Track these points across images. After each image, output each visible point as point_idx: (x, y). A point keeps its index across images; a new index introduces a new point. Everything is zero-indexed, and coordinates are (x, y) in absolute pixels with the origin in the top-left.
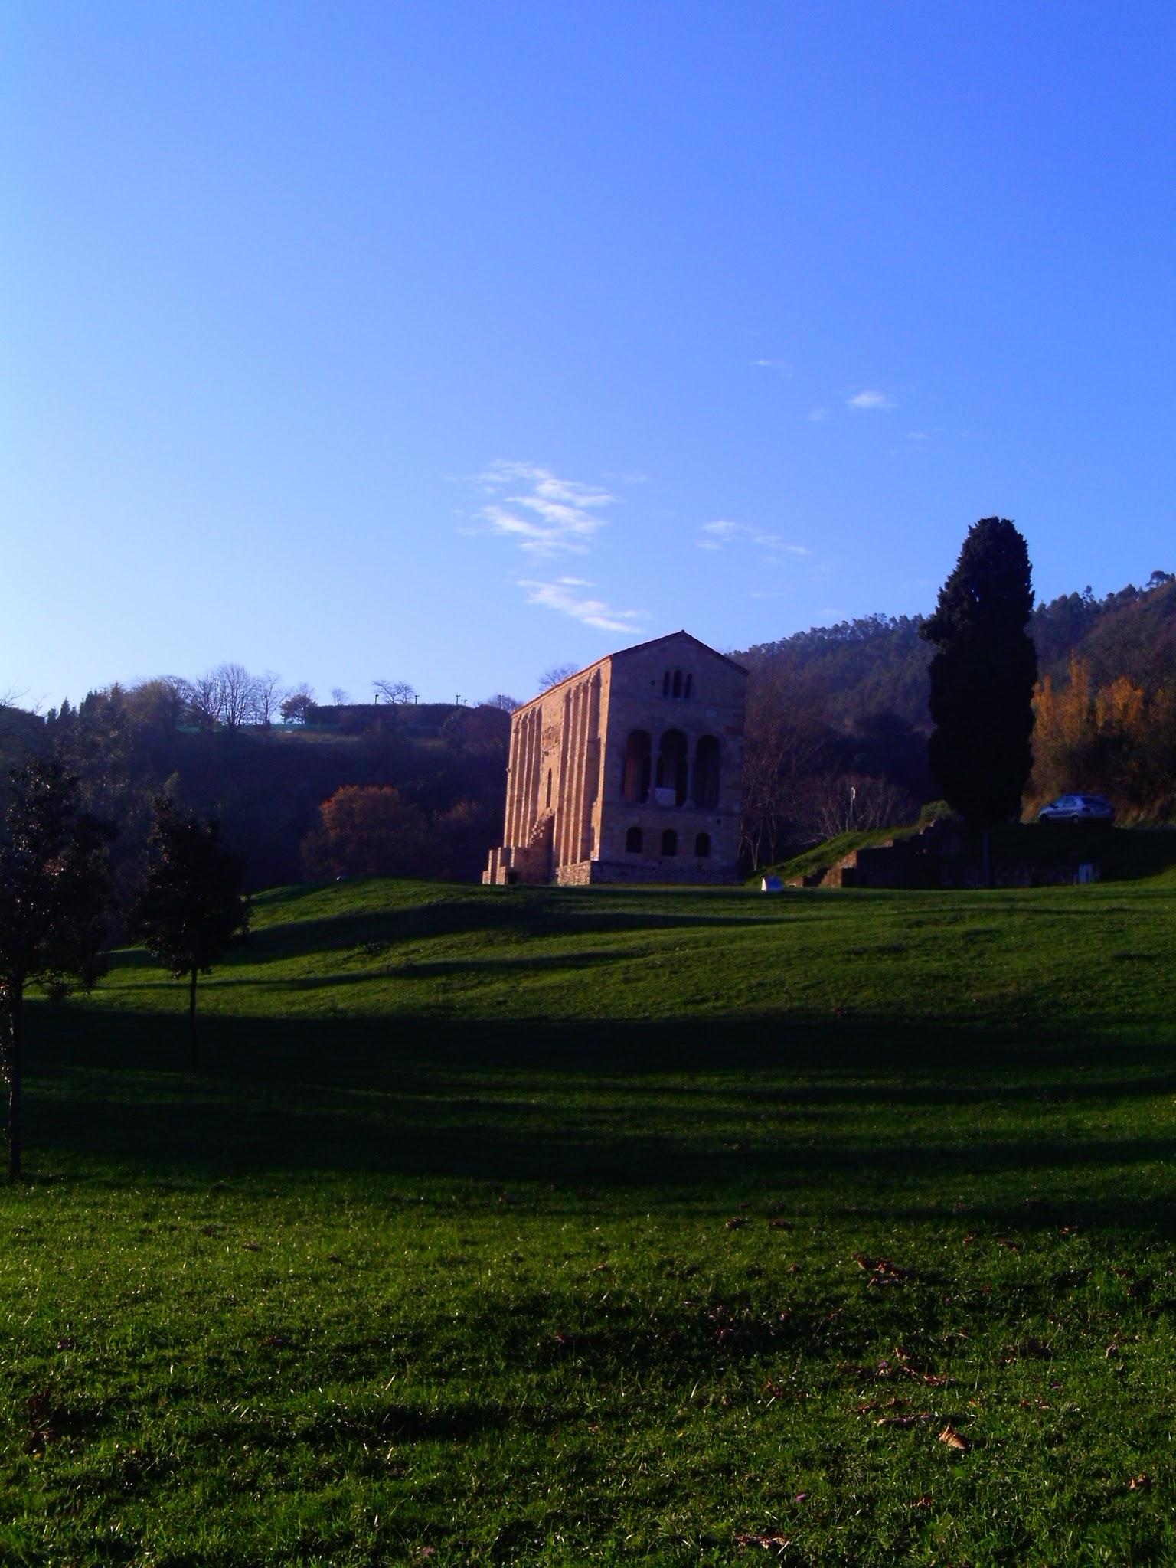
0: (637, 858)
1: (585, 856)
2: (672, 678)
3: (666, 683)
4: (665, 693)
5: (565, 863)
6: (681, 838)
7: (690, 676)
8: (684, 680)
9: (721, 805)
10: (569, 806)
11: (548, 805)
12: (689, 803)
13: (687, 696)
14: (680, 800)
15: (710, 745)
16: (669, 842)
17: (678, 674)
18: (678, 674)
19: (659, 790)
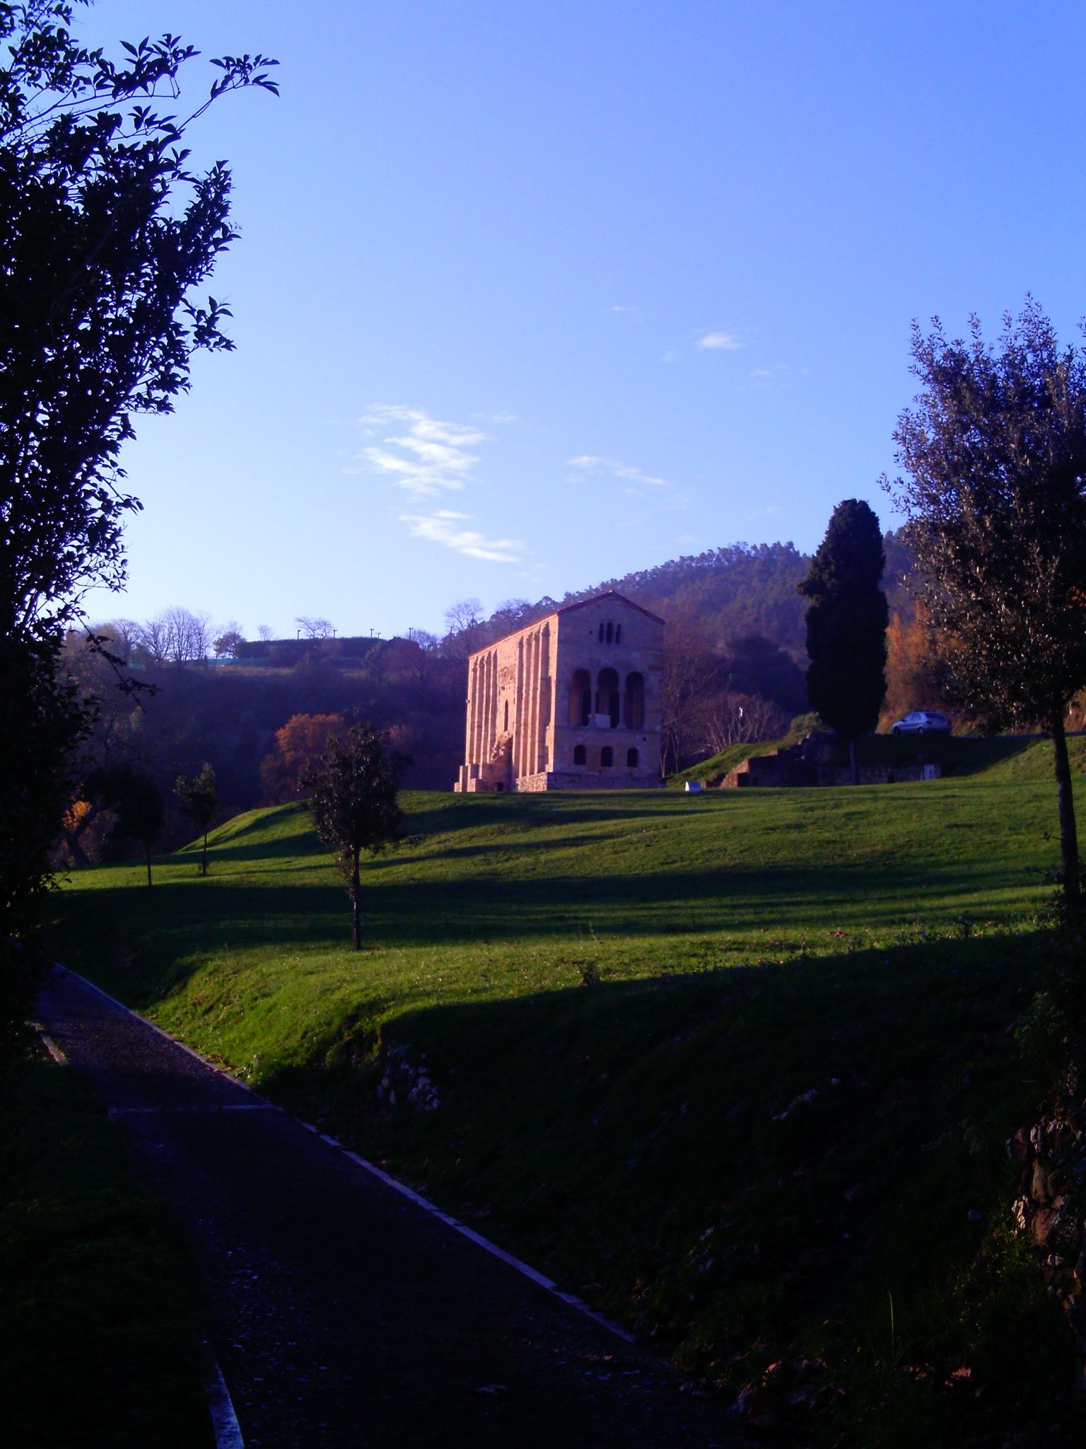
0: (582, 769)
1: (541, 769)
2: (605, 628)
3: (601, 632)
4: (601, 640)
5: (524, 774)
6: (615, 753)
7: (619, 626)
8: (615, 629)
9: (646, 727)
10: (526, 730)
11: (506, 729)
12: (621, 725)
13: (618, 641)
14: (614, 723)
15: (636, 679)
16: (607, 756)
17: (610, 625)
18: (610, 625)
19: (597, 716)
